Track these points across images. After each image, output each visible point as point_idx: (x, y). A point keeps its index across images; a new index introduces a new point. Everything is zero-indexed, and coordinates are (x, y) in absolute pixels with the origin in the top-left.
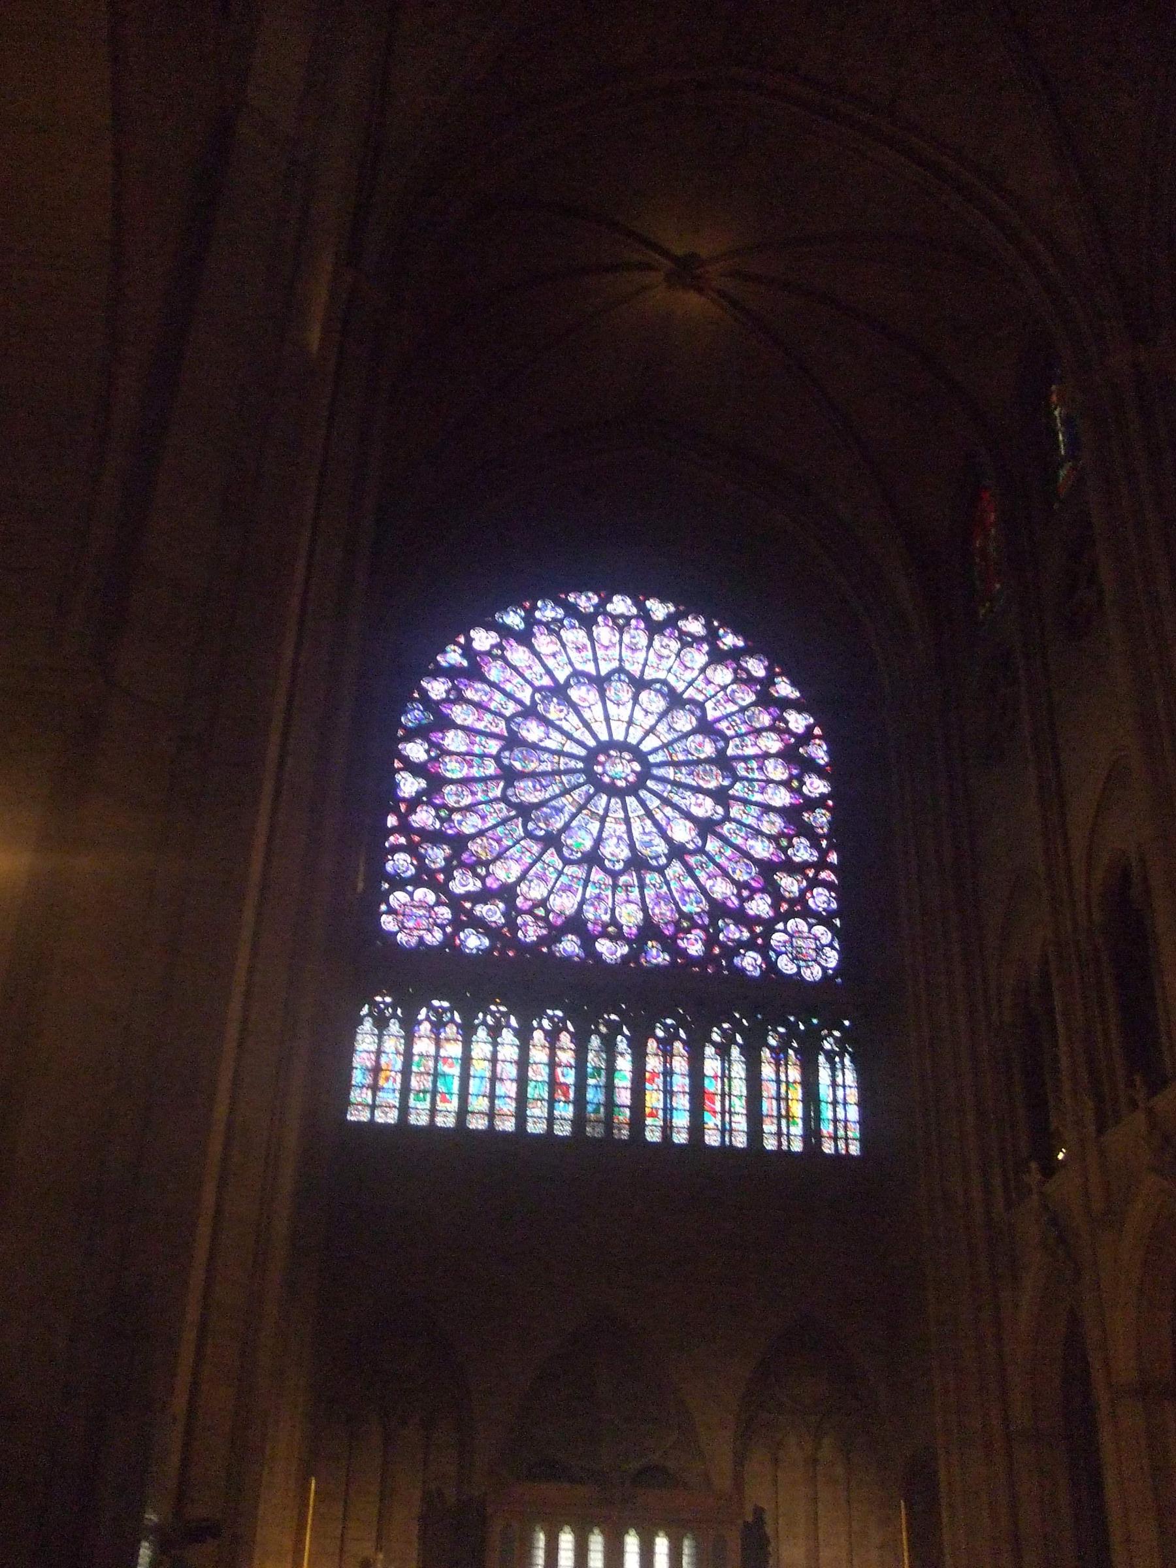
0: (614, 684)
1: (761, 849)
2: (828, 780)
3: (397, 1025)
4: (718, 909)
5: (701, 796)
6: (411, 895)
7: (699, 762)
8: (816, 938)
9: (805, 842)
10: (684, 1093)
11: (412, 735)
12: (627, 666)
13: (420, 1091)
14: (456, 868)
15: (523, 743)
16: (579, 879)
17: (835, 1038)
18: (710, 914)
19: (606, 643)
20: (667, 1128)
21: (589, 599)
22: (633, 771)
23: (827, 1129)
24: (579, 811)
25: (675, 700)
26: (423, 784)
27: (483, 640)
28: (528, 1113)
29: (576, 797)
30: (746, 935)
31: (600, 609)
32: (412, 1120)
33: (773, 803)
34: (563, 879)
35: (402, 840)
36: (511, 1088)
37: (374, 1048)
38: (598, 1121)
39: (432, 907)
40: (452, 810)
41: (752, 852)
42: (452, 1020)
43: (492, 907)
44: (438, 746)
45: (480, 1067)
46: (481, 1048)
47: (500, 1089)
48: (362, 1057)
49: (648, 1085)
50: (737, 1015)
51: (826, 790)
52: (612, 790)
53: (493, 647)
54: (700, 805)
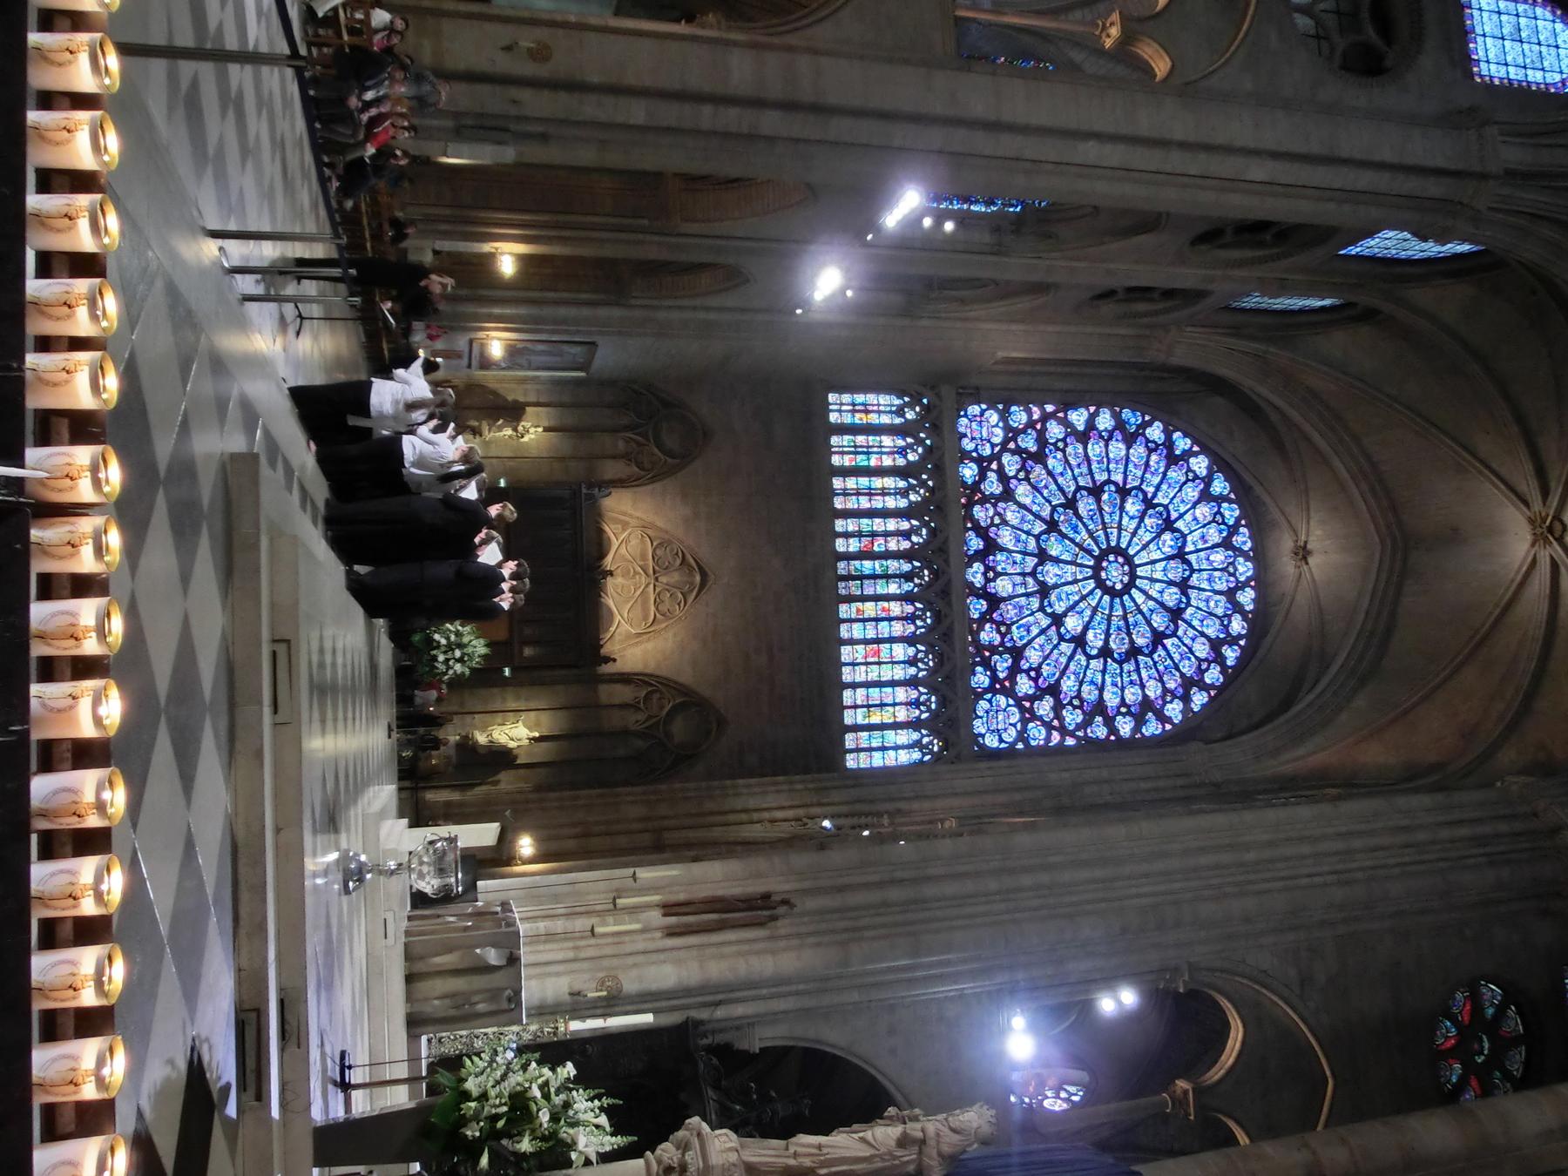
1: (1068, 685)
4: (1017, 653)
7: (1129, 634)
9: (1080, 719)
11: (1116, 416)
15: (1123, 501)
21: (1244, 543)
24: (1077, 545)
25: (1176, 614)
26: (1081, 428)
27: (1200, 464)
30: (1002, 676)
31: (1238, 551)
34: (1024, 536)
35: (1035, 417)
36: (864, 503)
40: (1064, 451)
44: (1110, 438)
45: (878, 483)
46: (889, 482)
48: (871, 398)
52: (1097, 569)
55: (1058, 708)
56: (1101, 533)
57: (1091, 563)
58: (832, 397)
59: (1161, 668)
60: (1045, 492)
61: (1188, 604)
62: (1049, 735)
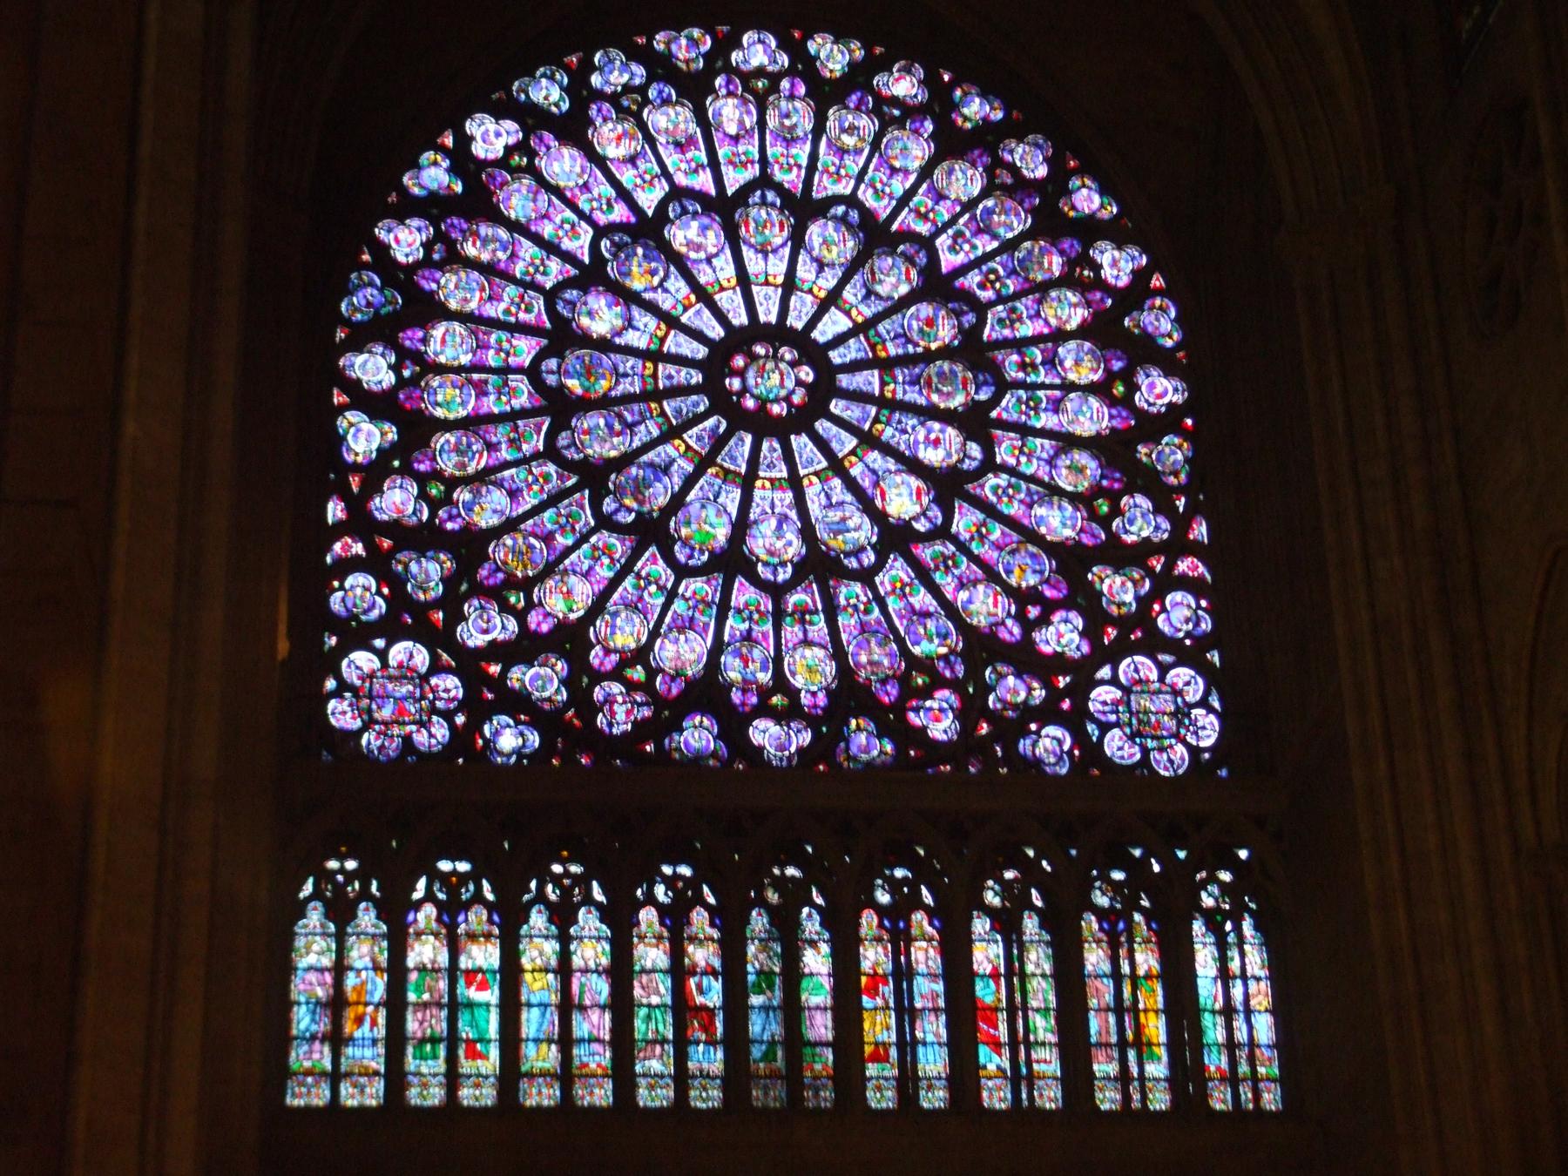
0: (753, 212)
1: (1058, 522)
2: (1182, 379)
3: (373, 914)
4: (981, 647)
5: (937, 426)
6: (382, 655)
7: (928, 357)
8: (1176, 692)
9: (1143, 502)
10: (936, 1010)
11: (360, 339)
12: (779, 176)
13: (423, 1041)
14: (467, 597)
15: (586, 340)
16: (709, 605)
17: (1221, 884)
18: (966, 656)
19: (732, 129)
20: (908, 1080)
21: (693, 43)
22: (799, 383)
23: (1215, 1061)
25: (875, 236)
27: (491, 137)
28: (638, 1068)
29: (692, 443)
30: (1039, 694)
32: (414, 1096)
33: (1078, 431)
34: (679, 606)
35: (358, 548)
37: (326, 961)
38: (773, 1075)
39: (425, 678)
40: (452, 483)
41: (1043, 530)
42: (478, 898)
43: (542, 671)
44: (418, 358)
45: (538, 988)
46: (539, 950)
47: (581, 1027)
49: (866, 1001)
50: (1031, 853)
51: (1178, 398)
52: (761, 424)
53: (509, 150)
54: (936, 443)
55: (1121, 556)
56: (668, 407)
57: (748, 439)
58: (307, 1095)
59: (1011, 286)
60: (564, 541)
61: (852, 201)
62: (1184, 583)
